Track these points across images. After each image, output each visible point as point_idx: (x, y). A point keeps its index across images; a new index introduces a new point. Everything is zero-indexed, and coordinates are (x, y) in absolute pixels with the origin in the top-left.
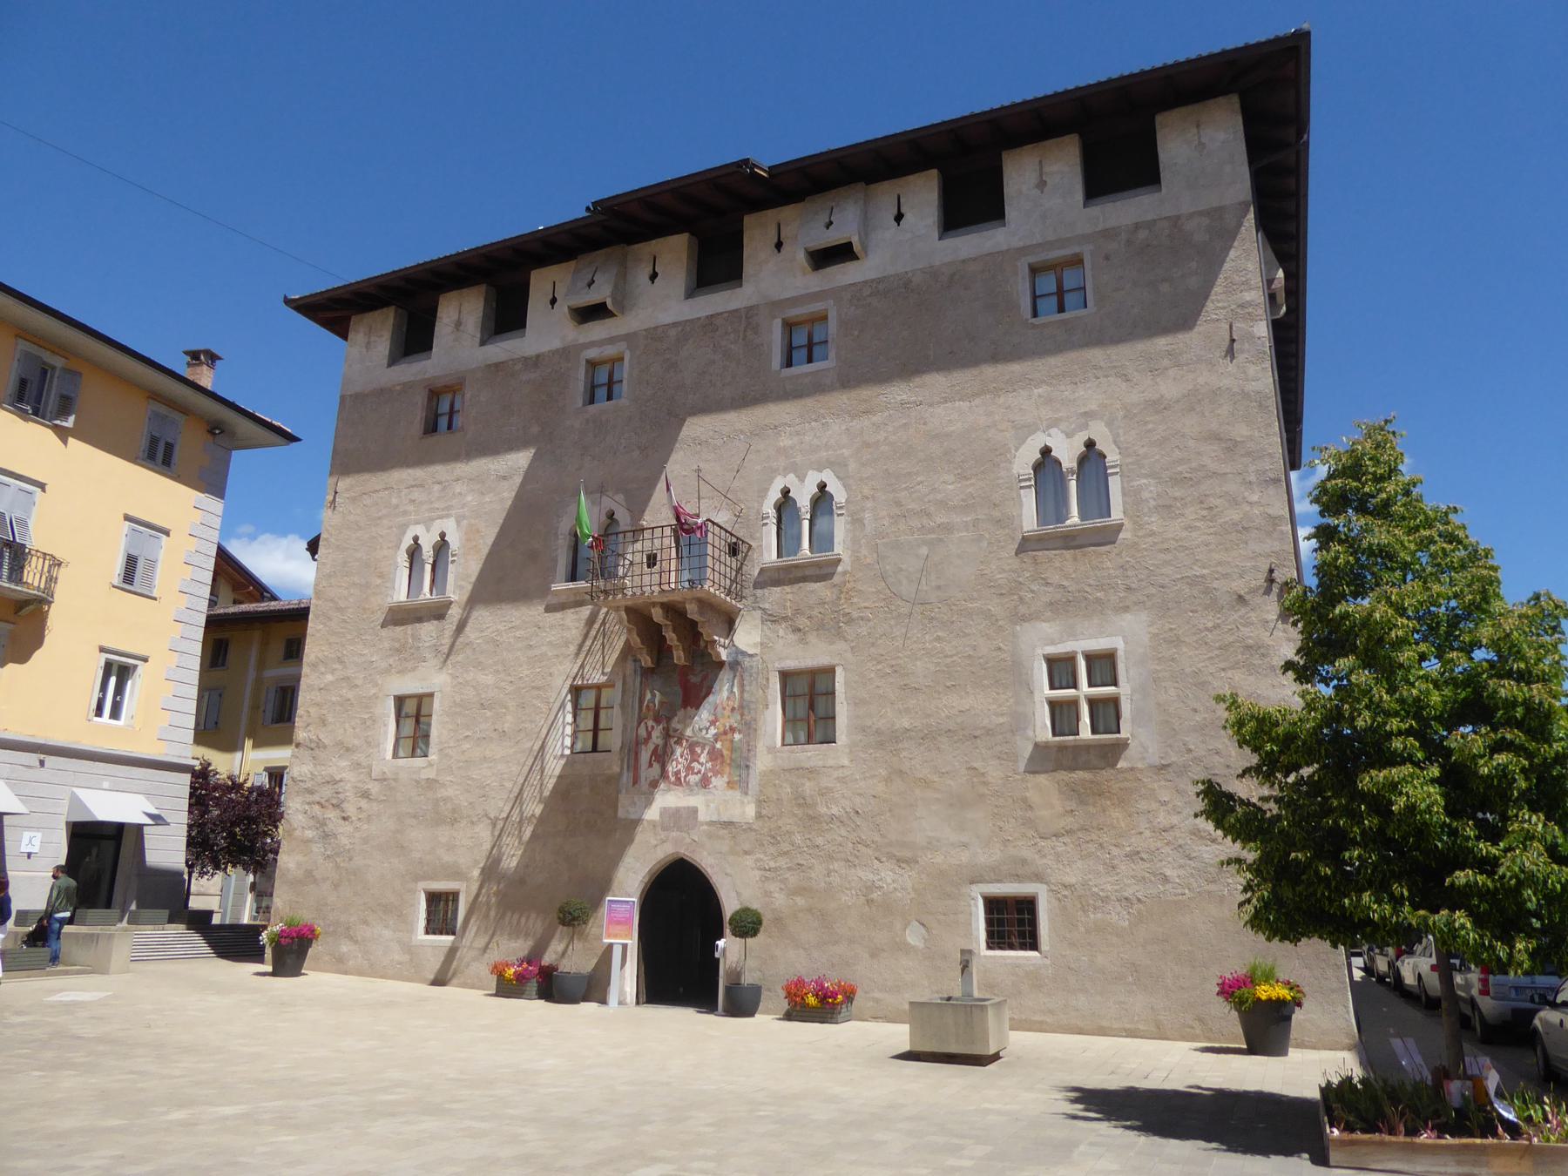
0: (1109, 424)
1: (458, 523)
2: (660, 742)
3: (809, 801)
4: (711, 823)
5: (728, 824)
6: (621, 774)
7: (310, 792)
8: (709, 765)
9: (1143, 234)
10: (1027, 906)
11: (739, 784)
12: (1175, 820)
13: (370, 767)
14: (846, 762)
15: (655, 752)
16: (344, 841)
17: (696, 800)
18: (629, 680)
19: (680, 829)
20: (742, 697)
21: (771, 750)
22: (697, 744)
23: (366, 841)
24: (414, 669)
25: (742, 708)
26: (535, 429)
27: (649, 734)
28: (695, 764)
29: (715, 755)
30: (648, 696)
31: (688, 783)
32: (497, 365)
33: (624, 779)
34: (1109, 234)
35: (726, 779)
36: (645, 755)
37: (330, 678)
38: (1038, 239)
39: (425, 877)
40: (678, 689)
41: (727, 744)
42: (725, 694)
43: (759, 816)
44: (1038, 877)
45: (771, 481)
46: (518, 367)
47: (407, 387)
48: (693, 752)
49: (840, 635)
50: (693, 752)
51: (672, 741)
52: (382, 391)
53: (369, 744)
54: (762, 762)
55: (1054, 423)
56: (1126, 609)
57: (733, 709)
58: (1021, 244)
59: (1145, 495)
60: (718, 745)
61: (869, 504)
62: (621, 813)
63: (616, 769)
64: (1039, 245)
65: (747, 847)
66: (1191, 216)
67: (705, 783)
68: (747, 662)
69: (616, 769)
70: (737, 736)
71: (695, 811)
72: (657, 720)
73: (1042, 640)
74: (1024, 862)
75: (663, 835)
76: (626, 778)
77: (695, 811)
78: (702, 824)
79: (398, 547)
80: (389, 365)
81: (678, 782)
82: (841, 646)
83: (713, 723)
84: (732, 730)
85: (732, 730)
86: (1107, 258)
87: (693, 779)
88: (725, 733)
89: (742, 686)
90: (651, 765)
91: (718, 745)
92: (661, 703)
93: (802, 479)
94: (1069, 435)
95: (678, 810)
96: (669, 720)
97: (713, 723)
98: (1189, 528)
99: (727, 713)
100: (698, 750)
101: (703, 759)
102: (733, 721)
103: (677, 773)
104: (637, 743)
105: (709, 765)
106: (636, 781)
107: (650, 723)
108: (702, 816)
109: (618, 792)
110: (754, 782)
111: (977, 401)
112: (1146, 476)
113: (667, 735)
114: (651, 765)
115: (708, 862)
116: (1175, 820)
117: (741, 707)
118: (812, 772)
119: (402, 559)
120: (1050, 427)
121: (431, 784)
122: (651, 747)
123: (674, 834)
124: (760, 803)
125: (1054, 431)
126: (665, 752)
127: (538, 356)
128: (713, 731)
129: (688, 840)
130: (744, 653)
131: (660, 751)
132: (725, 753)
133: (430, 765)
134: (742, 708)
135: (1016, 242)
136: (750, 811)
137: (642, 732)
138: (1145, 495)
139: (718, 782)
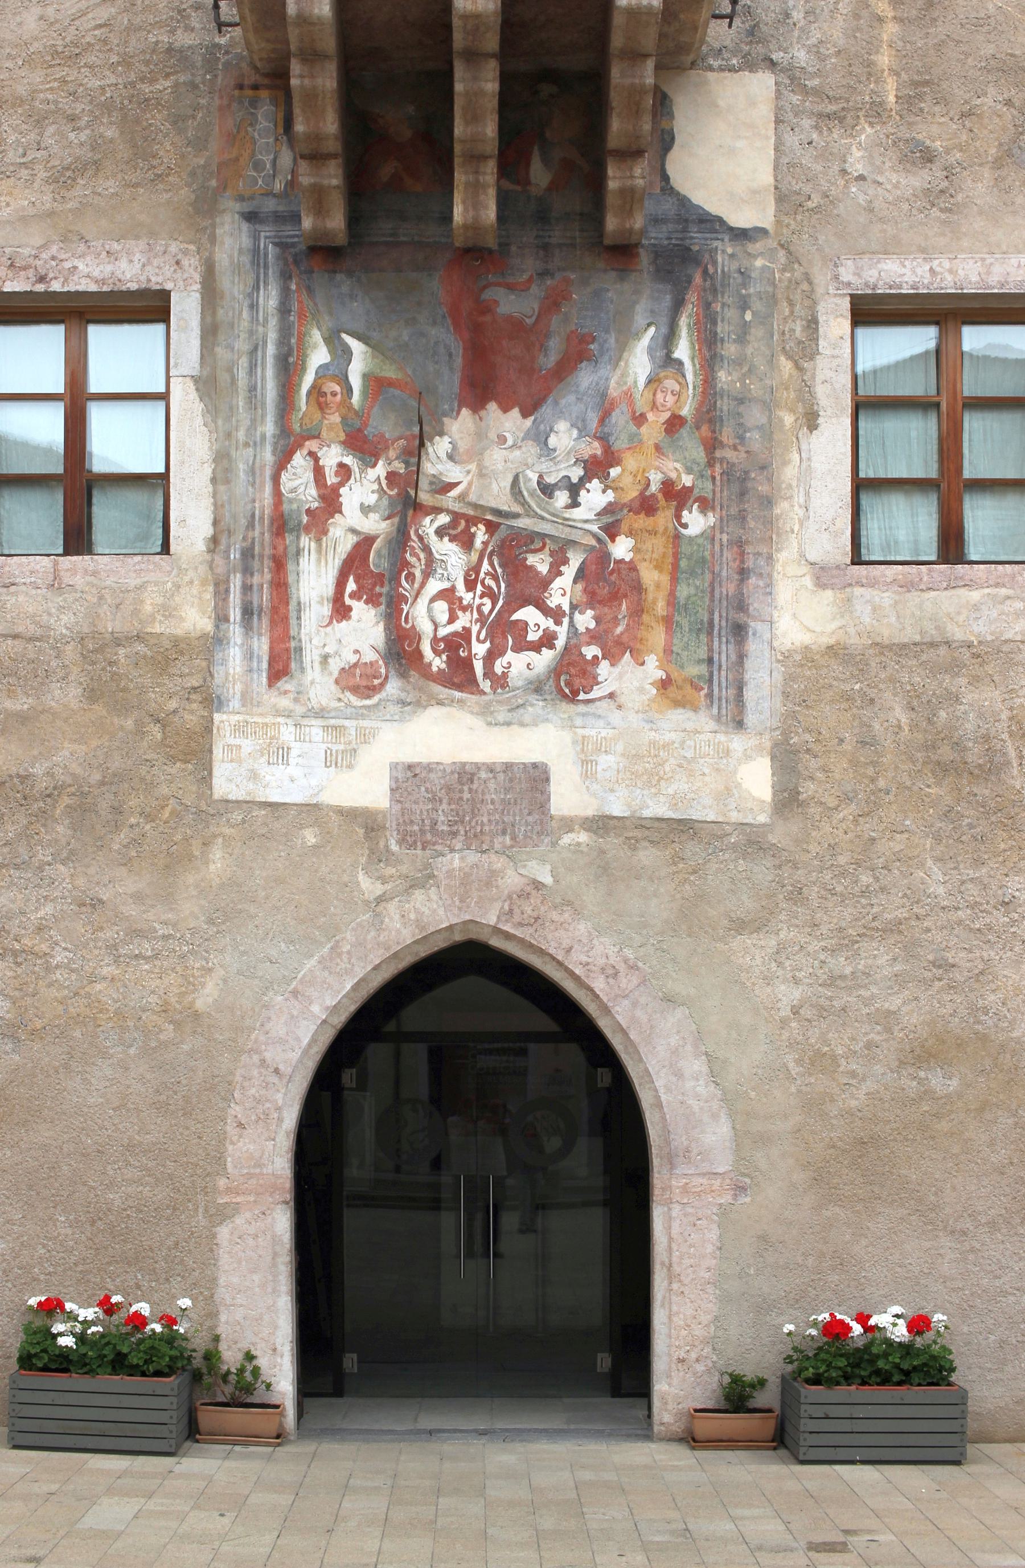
2: (376, 525)
3: (975, 755)
4: (601, 824)
5: (680, 829)
6: (217, 640)
8: (585, 620)
15: (355, 562)
17: (541, 739)
18: (233, 287)
19: (475, 839)
20: (708, 381)
21: (823, 576)
22: (531, 540)
25: (710, 421)
27: (331, 502)
28: (528, 614)
30: (319, 356)
31: (500, 682)
35: (653, 669)
36: (314, 578)
40: (446, 338)
41: (657, 546)
42: (639, 363)
43: (788, 800)
50: (515, 568)
51: (429, 526)
54: (797, 614)
57: (674, 424)
60: (621, 549)
62: (228, 781)
63: (195, 619)
65: (746, 904)
67: (571, 681)
68: (725, 255)
70: (696, 522)
71: (537, 777)
72: (362, 444)
76: (239, 660)
77: (537, 777)
78: (568, 824)
81: (460, 674)
83: (596, 468)
84: (677, 496)
85: (677, 496)
87: (520, 665)
88: (646, 505)
89: (708, 344)
90: (341, 611)
91: (621, 549)
92: (375, 384)
95: (466, 775)
96: (416, 450)
97: (596, 468)
99: (652, 430)
100: (540, 563)
101: (562, 591)
103: (454, 645)
104: (281, 524)
105: (585, 620)
106: (280, 668)
107: (332, 456)
108: (567, 797)
109: (212, 702)
110: (762, 681)
113: (406, 502)
114: (341, 611)
117: (709, 413)
122: (341, 537)
123: (454, 861)
124: (786, 760)
126: (400, 566)
128: (595, 497)
129: (511, 880)
130: (712, 224)
132: (650, 576)
134: (710, 421)
136: (757, 780)
137: (299, 483)
139: (629, 680)
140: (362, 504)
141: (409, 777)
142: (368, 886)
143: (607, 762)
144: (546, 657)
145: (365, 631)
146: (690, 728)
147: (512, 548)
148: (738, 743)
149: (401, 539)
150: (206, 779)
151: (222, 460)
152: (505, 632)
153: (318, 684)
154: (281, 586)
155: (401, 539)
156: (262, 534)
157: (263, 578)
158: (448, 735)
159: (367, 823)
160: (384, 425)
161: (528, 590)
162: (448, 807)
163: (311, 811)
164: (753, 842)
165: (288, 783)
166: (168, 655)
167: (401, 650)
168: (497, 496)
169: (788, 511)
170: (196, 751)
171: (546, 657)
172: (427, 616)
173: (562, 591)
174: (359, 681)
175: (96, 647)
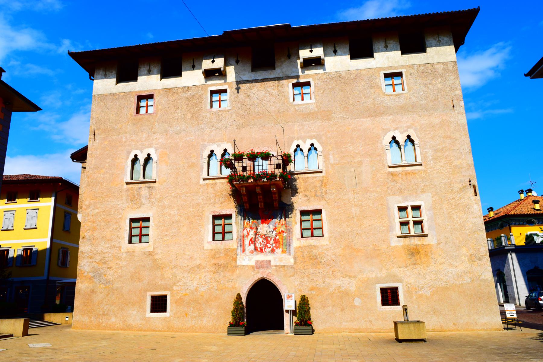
0: (415, 130)
1: (156, 150)
2: (253, 236)
3: (315, 257)
4: (276, 266)
5: (285, 266)
6: (237, 249)
7: (91, 258)
8: (274, 245)
9: (422, 68)
10: (395, 290)
11: (287, 251)
12: (443, 260)
13: (120, 247)
14: (328, 244)
15: (251, 240)
16: (110, 277)
19: (264, 268)
21: (298, 239)
22: (268, 237)
23: (120, 277)
24: (139, 207)
26: (189, 116)
27: (248, 234)
28: (268, 245)
29: (276, 241)
31: (266, 252)
32: (169, 89)
33: (239, 250)
34: (410, 66)
35: (281, 250)
36: (247, 242)
37: (97, 211)
38: (386, 65)
39: (150, 291)
41: (281, 237)
43: (295, 263)
44: (400, 281)
45: (293, 141)
46: (180, 90)
47: (127, 94)
48: (267, 240)
49: (323, 199)
50: (267, 240)
52: (114, 94)
53: (119, 238)
55: (396, 129)
56: (424, 192)
58: (381, 66)
59: (428, 155)
60: (277, 237)
61: (331, 152)
62: (239, 263)
63: (235, 247)
64: (386, 67)
65: (291, 274)
66: (438, 63)
67: (273, 251)
69: (235, 247)
70: (285, 234)
71: (269, 262)
72: (251, 228)
73: (397, 202)
74: (395, 276)
75: (257, 271)
76: (240, 250)
77: (269, 262)
78: (273, 266)
79: (128, 158)
80: (116, 84)
81: (262, 251)
82: (323, 202)
84: (283, 232)
86: (411, 74)
87: (267, 250)
88: (280, 233)
90: (250, 245)
91: (277, 237)
93: (305, 142)
94: (402, 133)
95: (262, 261)
97: (275, 229)
98: (442, 166)
100: (269, 239)
101: (272, 242)
102: (283, 228)
103: (261, 248)
104: (243, 237)
105: (274, 245)
106: (244, 251)
107: (249, 229)
108: (272, 263)
109: (236, 254)
111: (369, 119)
112: (428, 149)
113: (256, 234)
114: (250, 245)
115: (275, 279)
116: (443, 260)
118: (315, 247)
119: (129, 163)
120: (395, 130)
121: (150, 254)
122: (249, 238)
123: (261, 270)
124: (295, 258)
125: (396, 131)
126: (255, 240)
127: (188, 87)
128: (275, 232)
129: (267, 272)
131: (253, 240)
132: (281, 240)
133: (150, 246)
135: (379, 66)
136: (292, 261)
137: (245, 233)
138: (428, 155)
140: (252, 234)
141: (257, 262)
142: (253, 273)
143: (277, 259)
144: (270, 249)
145: (252, 246)
146: (285, 255)
147: (266, 238)
148: (290, 257)
149: (255, 237)
150: (236, 263)
151: (238, 230)
152: (266, 246)
153: (247, 252)
154: (243, 243)
155: (255, 237)
156: (242, 238)
157: (242, 242)
158: (260, 257)
159: (253, 267)
160: (254, 226)
161: (268, 242)
162: (261, 265)
163: (247, 266)
164: (292, 267)
165: (244, 263)
166: (233, 250)
167: (256, 249)
168: (265, 233)
169: (294, 233)
170: (235, 260)
171: (270, 249)
172: (258, 245)
173: (272, 242)
174: (252, 252)
175: (225, 250)
